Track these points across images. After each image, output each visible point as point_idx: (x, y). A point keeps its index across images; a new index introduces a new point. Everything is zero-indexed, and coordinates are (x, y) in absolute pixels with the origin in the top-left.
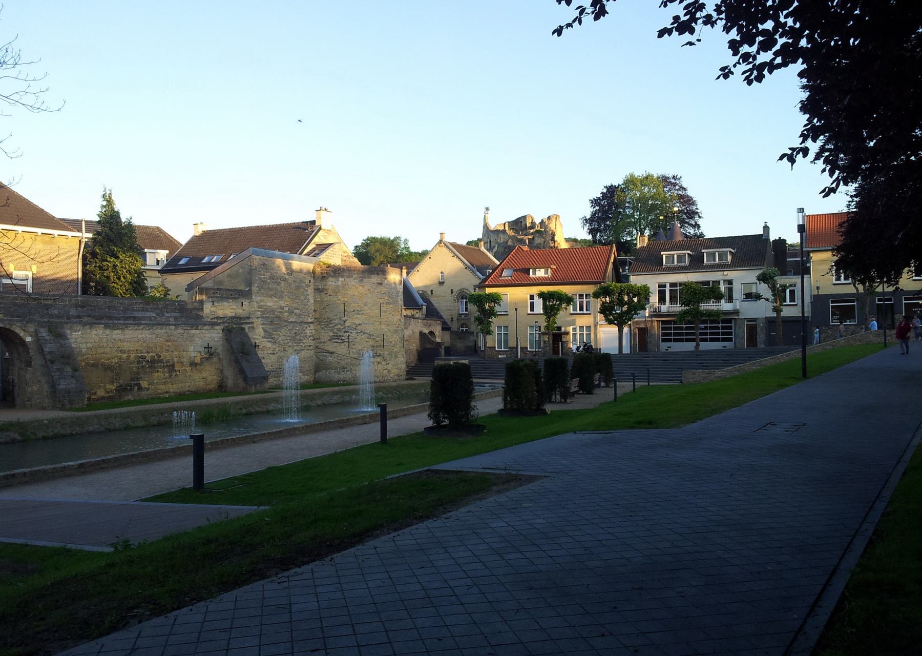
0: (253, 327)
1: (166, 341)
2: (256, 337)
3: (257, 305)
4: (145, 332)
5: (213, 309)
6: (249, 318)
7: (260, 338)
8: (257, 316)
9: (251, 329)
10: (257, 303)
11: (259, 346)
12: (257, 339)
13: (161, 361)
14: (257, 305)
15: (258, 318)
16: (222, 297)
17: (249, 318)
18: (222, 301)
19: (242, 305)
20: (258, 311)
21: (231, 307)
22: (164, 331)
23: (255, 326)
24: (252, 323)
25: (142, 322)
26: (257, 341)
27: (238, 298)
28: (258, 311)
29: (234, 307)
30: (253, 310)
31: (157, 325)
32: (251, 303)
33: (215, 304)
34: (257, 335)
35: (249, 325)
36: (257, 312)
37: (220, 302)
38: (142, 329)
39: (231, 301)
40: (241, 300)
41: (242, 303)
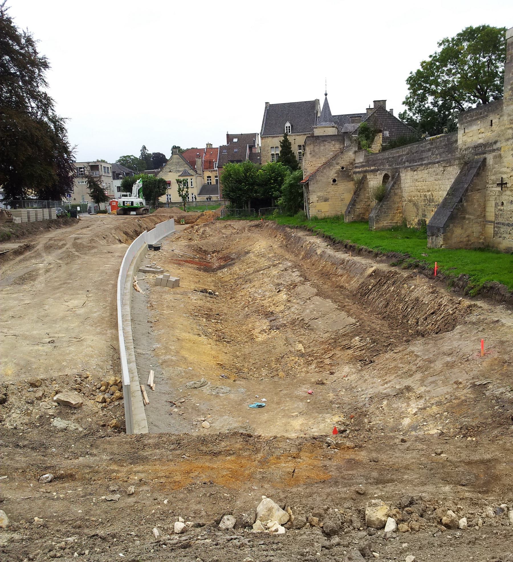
0: (500, 156)
1: (435, 180)
2: (504, 170)
3: (509, 118)
4: (426, 171)
5: (465, 138)
6: (496, 142)
7: (508, 170)
8: (507, 137)
9: (498, 159)
10: (509, 115)
11: (506, 183)
12: (505, 173)
13: (433, 201)
14: (509, 118)
15: (508, 140)
16: (472, 121)
17: (496, 142)
18: (471, 125)
19: (491, 125)
20: (508, 129)
21: (480, 131)
22: (433, 170)
23: (502, 153)
24: (499, 149)
25: (424, 162)
26: (505, 176)
27: (487, 116)
28: (508, 129)
29: (482, 130)
30: (503, 128)
31: (430, 163)
32: (501, 119)
33: (466, 131)
34: (505, 167)
35: (494, 154)
36: (508, 131)
37: (470, 127)
38: (424, 169)
39: (479, 122)
40: (491, 118)
41: (492, 121)
